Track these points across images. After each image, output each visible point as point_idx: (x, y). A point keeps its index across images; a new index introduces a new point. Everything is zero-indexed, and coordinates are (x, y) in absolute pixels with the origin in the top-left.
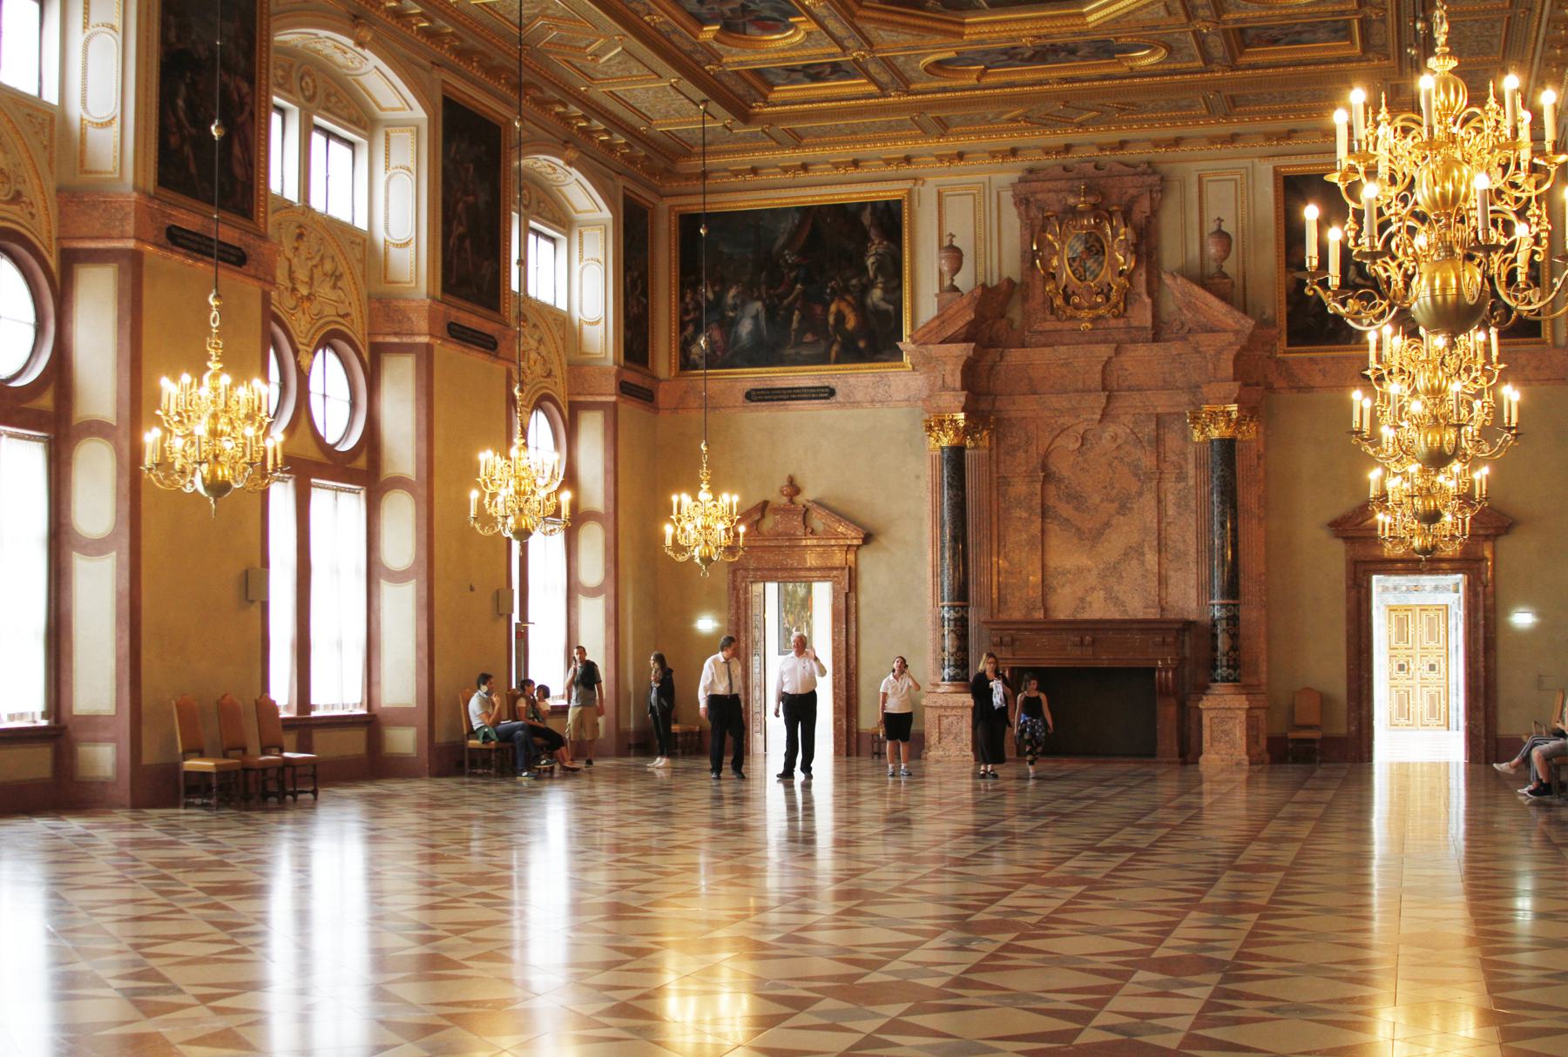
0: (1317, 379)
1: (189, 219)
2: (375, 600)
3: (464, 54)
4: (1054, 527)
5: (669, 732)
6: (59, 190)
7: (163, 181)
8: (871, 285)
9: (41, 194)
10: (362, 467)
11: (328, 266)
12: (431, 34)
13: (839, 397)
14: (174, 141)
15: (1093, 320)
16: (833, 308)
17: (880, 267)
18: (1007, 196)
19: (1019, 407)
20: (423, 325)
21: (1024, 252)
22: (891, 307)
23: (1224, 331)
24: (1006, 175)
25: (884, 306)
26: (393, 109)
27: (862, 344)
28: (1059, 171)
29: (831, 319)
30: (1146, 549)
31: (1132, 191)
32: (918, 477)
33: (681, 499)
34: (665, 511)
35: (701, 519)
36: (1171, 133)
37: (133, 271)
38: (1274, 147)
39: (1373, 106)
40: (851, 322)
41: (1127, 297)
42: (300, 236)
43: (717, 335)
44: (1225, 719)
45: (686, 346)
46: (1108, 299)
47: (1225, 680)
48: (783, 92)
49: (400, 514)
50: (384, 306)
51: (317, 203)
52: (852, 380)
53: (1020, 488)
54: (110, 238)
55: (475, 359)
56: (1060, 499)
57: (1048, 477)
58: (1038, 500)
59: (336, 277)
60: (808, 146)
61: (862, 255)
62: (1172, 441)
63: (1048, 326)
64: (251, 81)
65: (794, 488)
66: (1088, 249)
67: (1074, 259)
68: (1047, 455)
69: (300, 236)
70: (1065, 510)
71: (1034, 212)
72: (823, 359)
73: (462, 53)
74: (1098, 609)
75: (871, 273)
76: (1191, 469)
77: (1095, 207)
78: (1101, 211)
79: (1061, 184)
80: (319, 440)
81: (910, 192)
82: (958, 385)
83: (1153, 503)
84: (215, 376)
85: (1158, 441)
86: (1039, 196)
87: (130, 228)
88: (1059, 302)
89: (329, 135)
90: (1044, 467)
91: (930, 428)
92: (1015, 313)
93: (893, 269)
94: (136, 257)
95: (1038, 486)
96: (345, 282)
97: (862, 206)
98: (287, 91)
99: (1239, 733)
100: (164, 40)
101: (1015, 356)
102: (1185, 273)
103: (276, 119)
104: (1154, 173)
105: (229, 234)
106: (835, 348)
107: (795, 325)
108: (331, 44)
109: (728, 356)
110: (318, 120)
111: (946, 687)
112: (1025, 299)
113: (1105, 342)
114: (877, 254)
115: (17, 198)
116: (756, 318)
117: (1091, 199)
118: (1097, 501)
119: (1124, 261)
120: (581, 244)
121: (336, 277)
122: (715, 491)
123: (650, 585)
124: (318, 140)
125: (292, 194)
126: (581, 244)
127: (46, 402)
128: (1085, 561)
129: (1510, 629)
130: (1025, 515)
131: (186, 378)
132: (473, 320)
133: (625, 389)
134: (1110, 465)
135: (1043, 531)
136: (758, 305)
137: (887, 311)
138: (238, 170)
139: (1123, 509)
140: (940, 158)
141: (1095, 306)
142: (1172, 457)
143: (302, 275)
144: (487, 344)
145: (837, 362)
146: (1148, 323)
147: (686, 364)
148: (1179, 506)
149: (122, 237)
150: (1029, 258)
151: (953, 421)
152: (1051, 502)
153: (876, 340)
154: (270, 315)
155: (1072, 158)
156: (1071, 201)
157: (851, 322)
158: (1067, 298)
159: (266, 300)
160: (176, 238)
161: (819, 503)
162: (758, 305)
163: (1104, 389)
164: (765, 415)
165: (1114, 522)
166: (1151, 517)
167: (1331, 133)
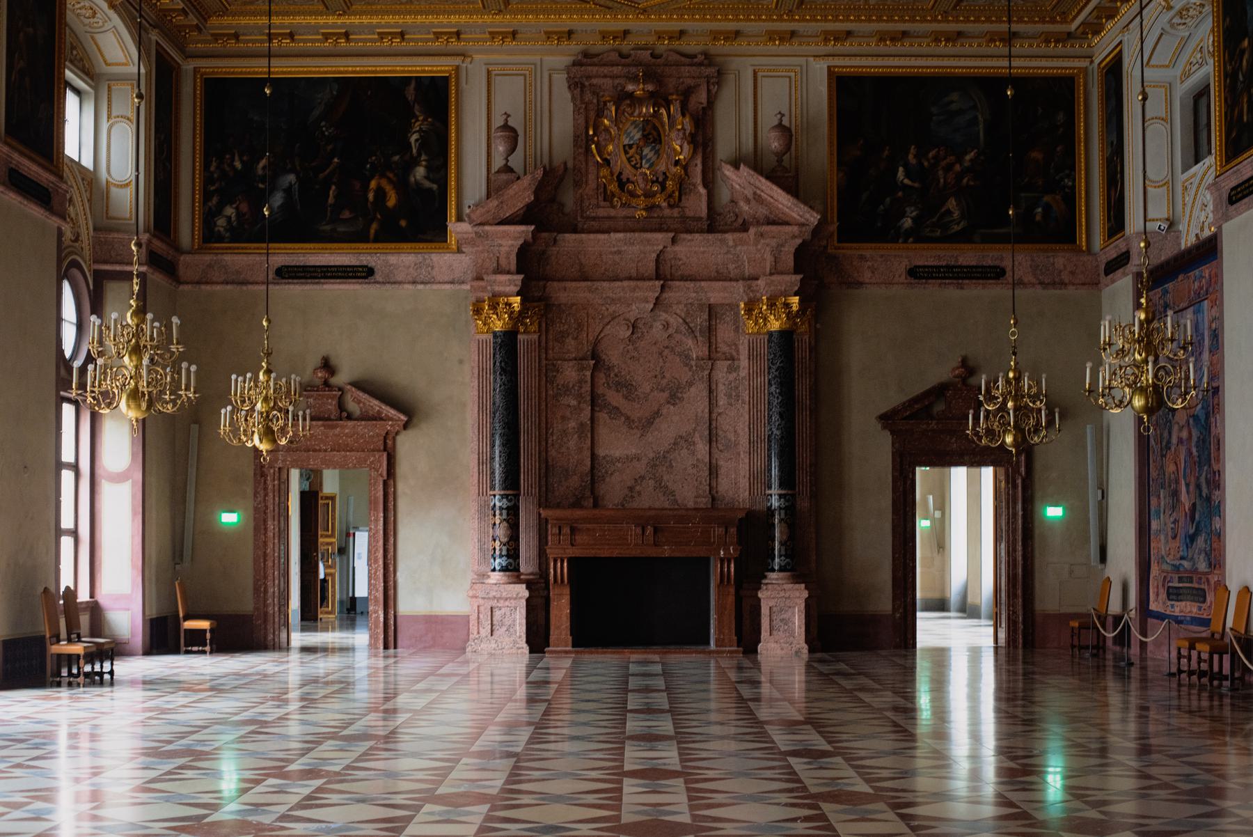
0: (867, 276)
4: (602, 416)
8: (415, 162)
13: (378, 276)
15: (647, 209)
16: (373, 184)
17: (424, 144)
18: (561, 80)
19: (567, 293)
21: (576, 137)
22: (435, 187)
23: (787, 223)
24: (558, 59)
25: (427, 184)
27: (403, 223)
28: (614, 57)
29: (371, 196)
30: (697, 438)
31: (689, 82)
32: (461, 362)
36: (732, 26)
38: (830, 47)
40: (392, 201)
41: (683, 186)
43: (244, 207)
44: (784, 608)
45: (209, 219)
46: (663, 187)
47: (781, 570)
52: (393, 259)
53: (569, 373)
56: (609, 388)
58: (587, 387)
60: (355, 14)
61: (407, 129)
62: (724, 332)
63: (601, 212)
66: (645, 137)
67: (630, 146)
68: (597, 342)
70: (615, 398)
71: (588, 96)
72: (359, 237)
75: (414, 151)
76: (744, 362)
77: (652, 95)
78: (659, 99)
79: (616, 70)
81: (458, 68)
82: (513, 267)
83: (705, 393)
85: (710, 331)
86: (595, 81)
88: (613, 187)
90: (595, 355)
91: (478, 311)
93: (439, 148)
95: (588, 373)
97: (407, 80)
99: (797, 620)
101: (569, 240)
102: (757, 162)
104: (710, 65)
106: (374, 226)
107: (331, 200)
109: (251, 232)
111: (496, 577)
112: (577, 184)
113: (660, 230)
114: (420, 131)
116: (288, 191)
117: (650, 87)
118: (646, 387)
119: (679, 147)
120: (109, 101)
126: (109, 101)
129: (1043, 520)
130: (573, 403)
134: (661, 354)
135: (592, 419)
136: (292, 178)
137: (430, 190)
140: (493, 35)
141: (653, 195)
142: (723, 348)
145: (376, 240)
146: (703, 211)
147: (210, 236)
148: (730, 396)
150: (582, 142)
151: (509, 304)
152: (600, 391)
153: (422, 221)
155: (626, 46)
156: (630, 87)
157: (392, 201)
158: (622, 185)
162: (292, 178)
163: (658, 278)
164: (295, 290)
165: (664, 411)
166: (702, 406)
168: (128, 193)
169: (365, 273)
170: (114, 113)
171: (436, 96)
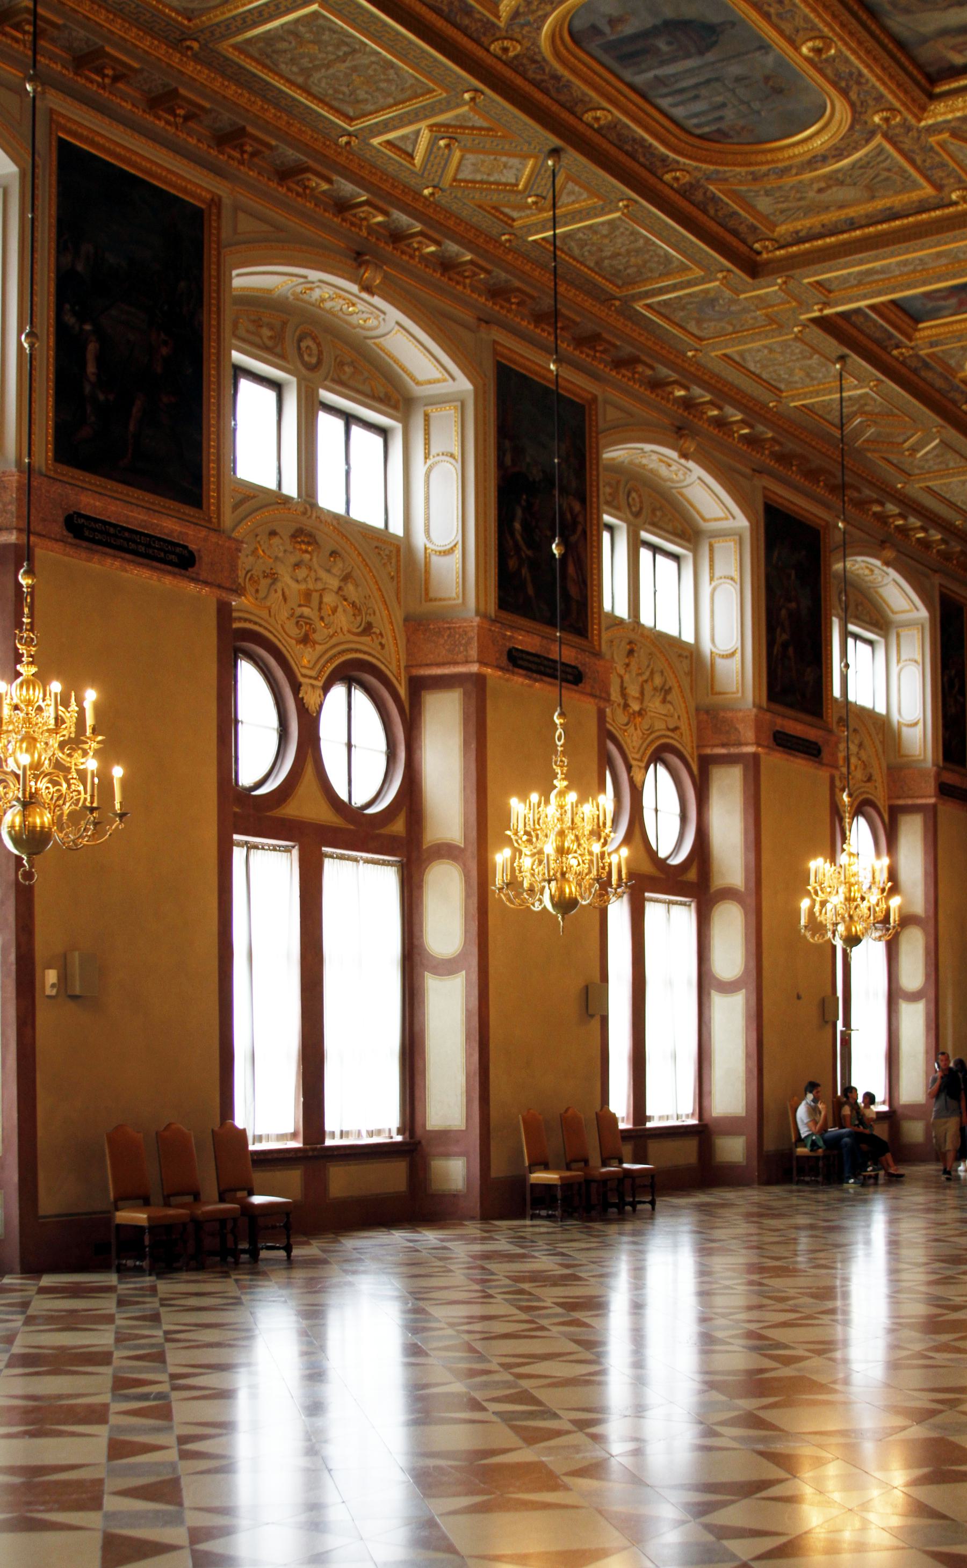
1: (528, 639)
2: (705, 1011)
3: (783, 458)
6: (407, 620)
7: (503, 604)
9: (390, 625)
10: (691, 879)
11: (658, 681)
12: (752, 441)
14: (512, 563)
20: (750, 735)
26: (716, 520)
37: (477, 692)
42: (631, 652)
49: (730, 926)
50: (712, 718)
51: (646, 619)
54: (456, 663)
55: (799, 765)
64: (583, 500)
69: (631, 652)
73: (783, 458)
80: (652, 854)
84: (562, 794)
87: (473, 653)
89: (655, 549)
94: (479, 681)
96: (674, 696)
98: (616, 510)
100: (500, 464)
103: (606, 536)
105: (569, 655)
108: (656, 458)
110: (645, 535)
115: (367, 629)
120: (898, 645)
124: (645, 555)
125: (622, 611)
126: (898, 645)
127: (398, 827)
131: (534, 797)
132: (797, 727)
138: (573, 591)
143: (633, 691)
144: (810, 750)
149: (467, 662)
154: (605, 735)
160: (517, 660)
168: (918, 731)
170: (903, 657)
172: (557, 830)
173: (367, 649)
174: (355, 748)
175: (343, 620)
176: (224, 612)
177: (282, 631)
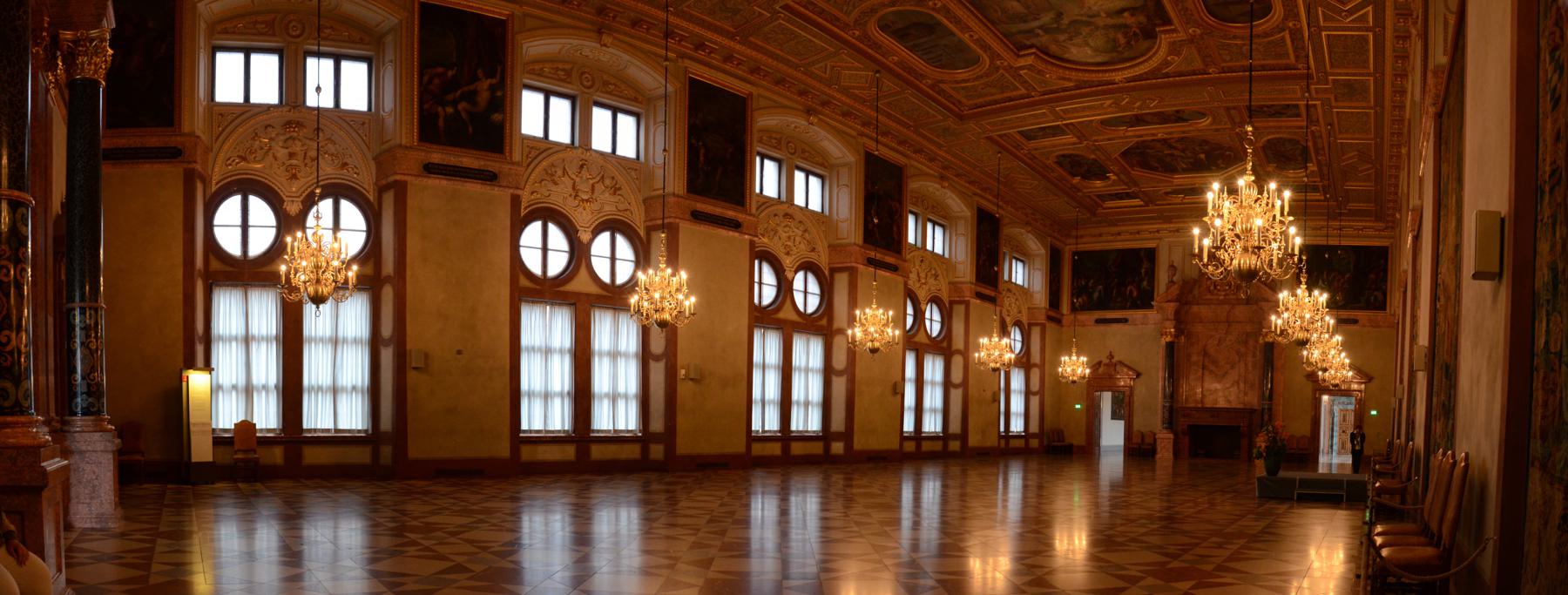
5: (1057, 448)
9: (822, 247)
33: (1065, 359)
34: (1059, 363)
35: (1074, 366)
39: (1222, 191)
48: (1109, 204)
53: (1194, 358)
55: (987, 305)
57: (1205, 354)
59: (936, 276)
65: (1111, 356)
72: (1124, 308)
74: (1222, 404)
92: (1196, 292)
101: (1195, 308)
105: (890, 260)
115: (813, 250)
121: (936, 276)
122: (1078, 356)
123: (1046, 391)
127: (824, 322)
128: (1218, 386)
132: (987, 292)
133: (1049, 318)
139: (1232, 367)
144: (992, 300)
153: (1144, 300)
159: (906, 284)
160: (871, 262)
161: (1121, 363)
164: (1102, 328)
167: (1206, 203)
169: (1125, 321)
171: (1151, 254)
172: (873, 324)
173: (813, 257)
174: (807, 294)
175: (802, 246)
176: (752, 244)
177: (779, 251)
